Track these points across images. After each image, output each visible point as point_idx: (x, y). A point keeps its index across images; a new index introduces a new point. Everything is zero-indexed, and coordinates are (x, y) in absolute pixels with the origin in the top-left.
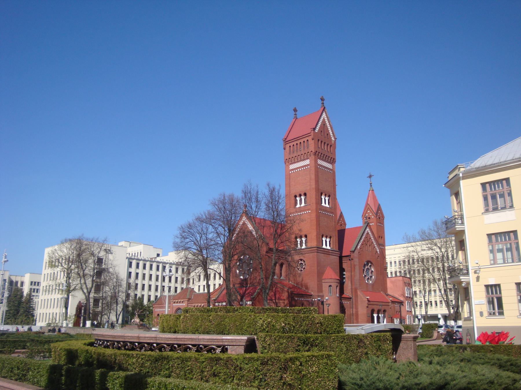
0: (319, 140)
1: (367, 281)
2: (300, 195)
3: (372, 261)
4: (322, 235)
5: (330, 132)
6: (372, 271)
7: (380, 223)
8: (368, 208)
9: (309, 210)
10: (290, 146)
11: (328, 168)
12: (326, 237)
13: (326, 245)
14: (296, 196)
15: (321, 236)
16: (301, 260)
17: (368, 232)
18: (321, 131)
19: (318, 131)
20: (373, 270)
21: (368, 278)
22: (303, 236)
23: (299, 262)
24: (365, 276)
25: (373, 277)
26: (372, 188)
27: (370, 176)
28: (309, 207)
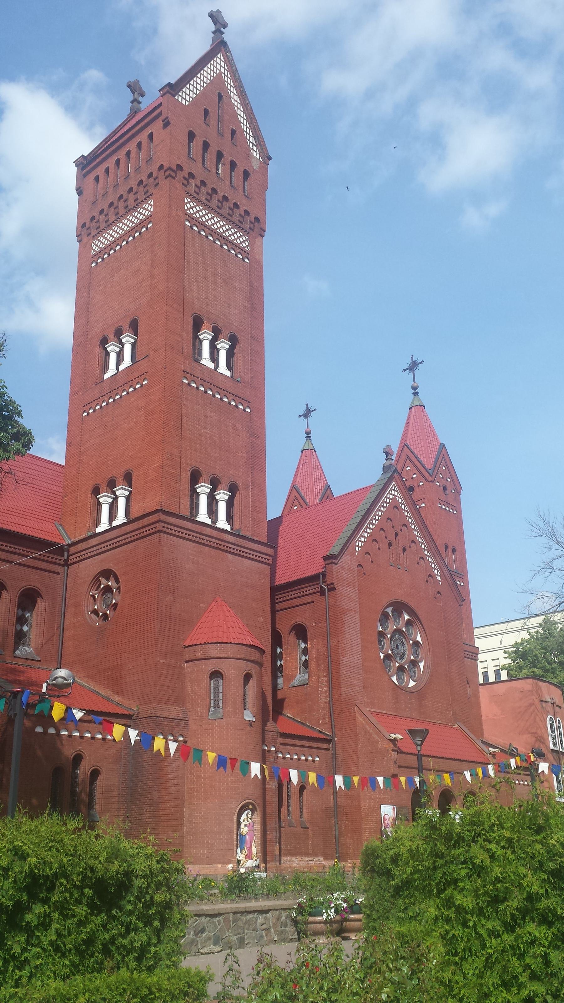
0: (191, 136)
1: (394, 679)
2: (119, 333)
3: (412, 605)
4: (189, 469)
5: (245, 127)
6: (416, 643)
7: (447, 503)
8: (408, 458)
9: (143, 376)
10: (97, 179)
11: (231, 242)
12: (215, 484)
13: (212, 511)
14: (104, 341)
15: (186, 478)
16: (107, 573)
17: (394, 500)
18: (206, 112)
19: (191, 104)
20: (419, 639)
21: (401, 669)
22: (120, 479)
23: (100, 585)
24: (388, 657)
25: (422, 665)
26: (419, 400)
27: (413, 367)
28: (143, 366)
